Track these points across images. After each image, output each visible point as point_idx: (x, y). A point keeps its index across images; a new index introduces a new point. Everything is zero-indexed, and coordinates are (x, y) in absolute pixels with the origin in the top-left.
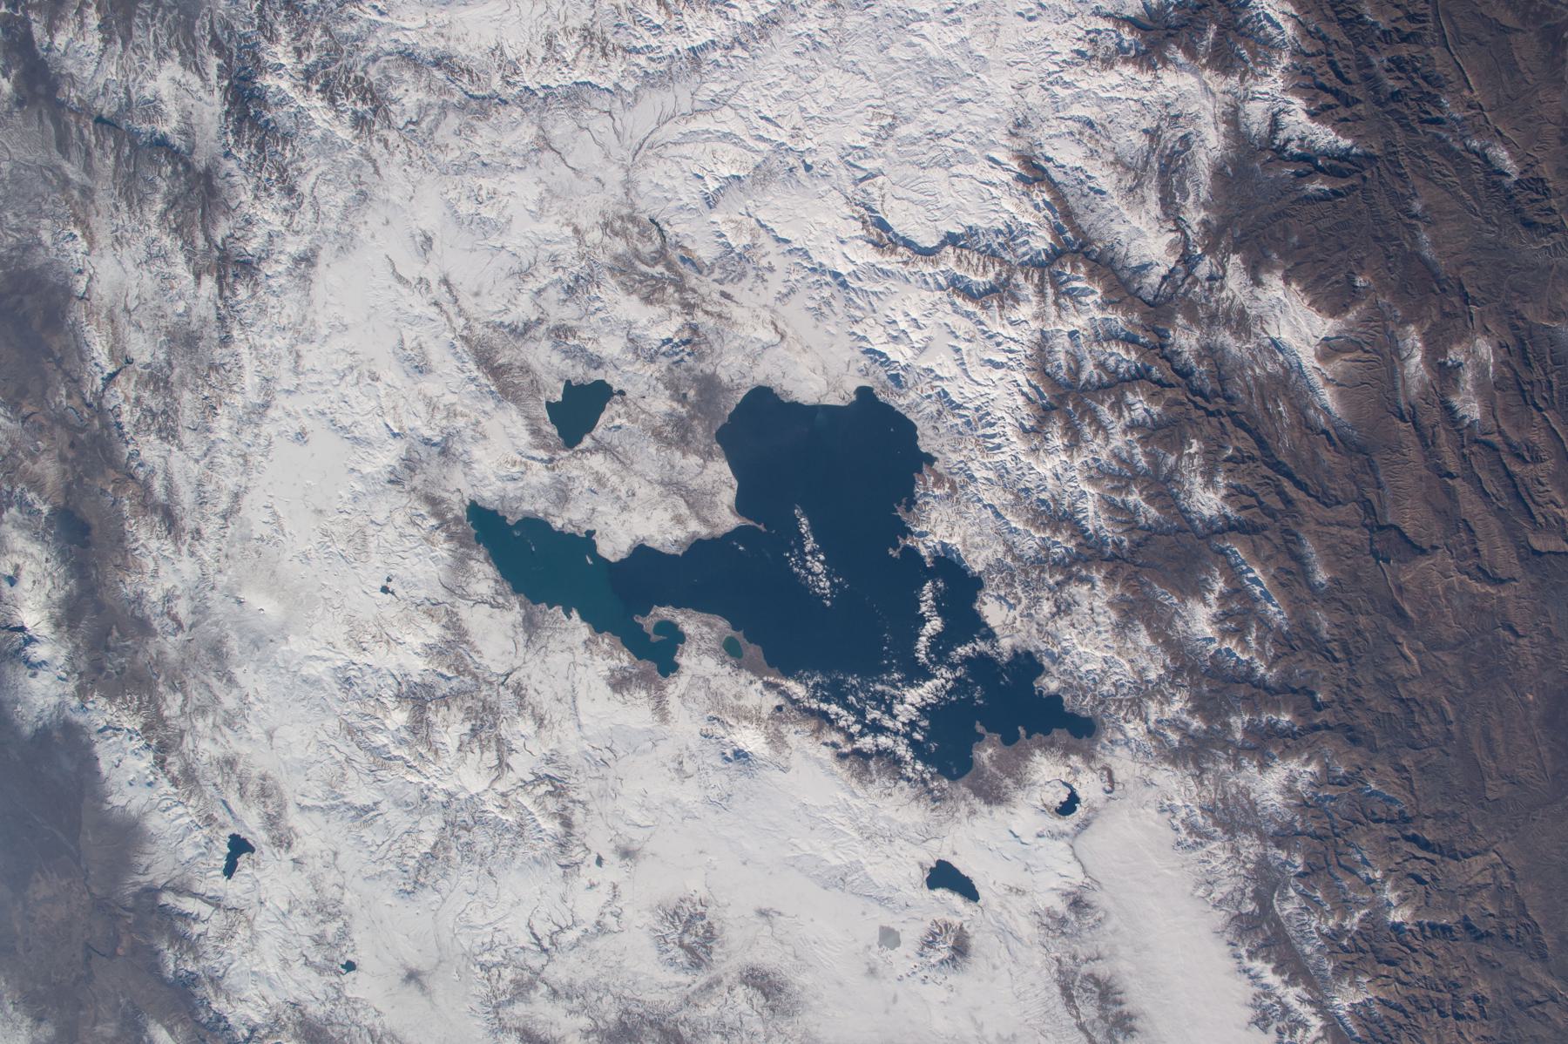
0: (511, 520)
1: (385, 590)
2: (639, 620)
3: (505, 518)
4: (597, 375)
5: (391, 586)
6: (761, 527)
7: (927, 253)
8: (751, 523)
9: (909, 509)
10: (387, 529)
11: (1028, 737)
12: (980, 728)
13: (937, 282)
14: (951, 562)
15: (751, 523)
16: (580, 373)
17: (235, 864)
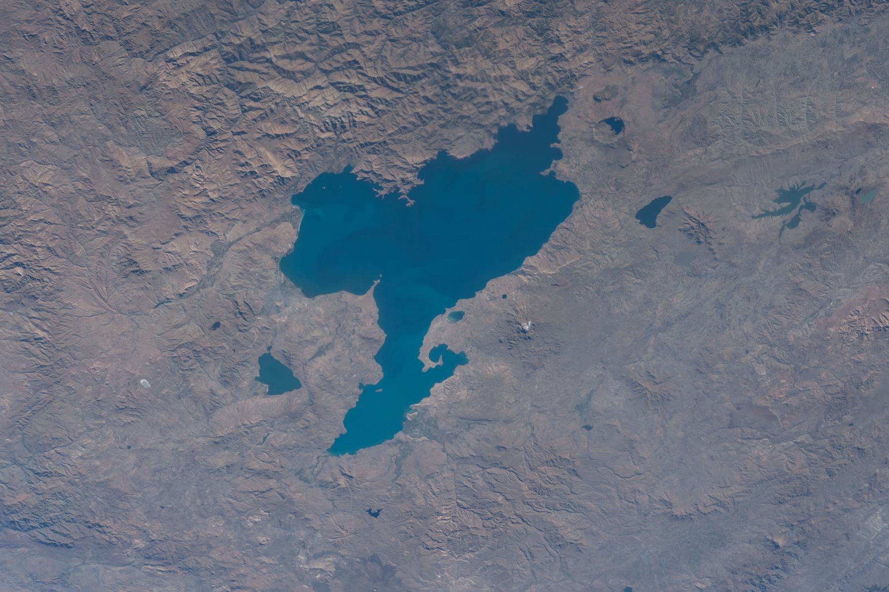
0: (345, 431)
2: (425, 369)
3: (341, 435)
6: (377, 282)
8: (373, 288)
9: (381, 188)
11: (559, 142)
12: (546, 173)
14: (423, 169)
15: (373, 288)
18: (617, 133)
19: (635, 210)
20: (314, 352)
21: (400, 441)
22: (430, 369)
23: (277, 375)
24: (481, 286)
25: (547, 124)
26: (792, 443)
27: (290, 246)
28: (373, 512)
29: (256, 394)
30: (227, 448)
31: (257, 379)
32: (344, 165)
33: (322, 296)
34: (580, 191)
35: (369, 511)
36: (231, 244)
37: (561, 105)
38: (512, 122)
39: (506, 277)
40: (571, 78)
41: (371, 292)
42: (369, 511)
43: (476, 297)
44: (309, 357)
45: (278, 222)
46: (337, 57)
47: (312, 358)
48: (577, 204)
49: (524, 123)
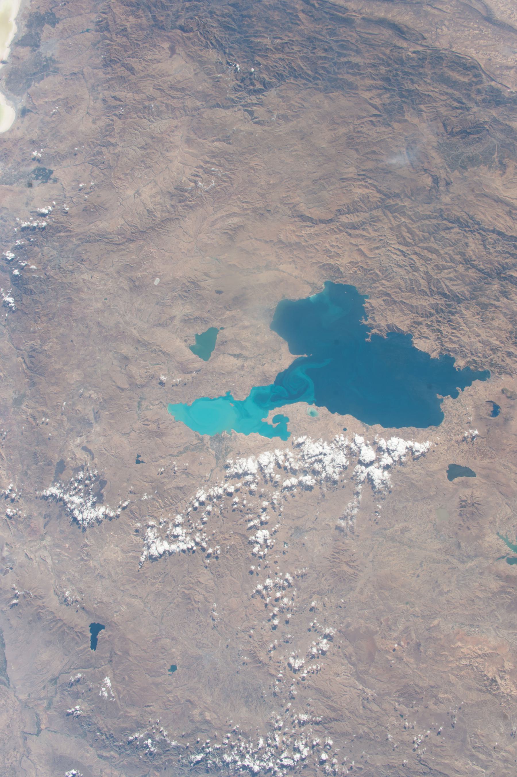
1: (138, 462)
2: (264, 420)
4: (210, 326)
5: (139, 459)
6: (305, 356)
7: (331, 221)
9: (366, 320)
10: (132, 434)
11: (463, 390)
12: (439, 397)
13: (339, 229)
15: (300, 356)
16: (201, 329)
17: (97, 639)
18: (492, 416)
19: (452, 462)
20: (236, 353)
21: (202, 440)
22: (266, 423)
23: (206, 345)
24: (342, 413)
25: (466, 378)
26: (361, 687)
27: (297, 298)
28: (139, 459)
29: (186, 341)
30: (137, 349)
31: (197, 335)
32: (366, 293)
33: (276, 334)
34: (442, 423)
35: (139, 456)
36: (278, 270)
37: (484, 376)
38: (456, 358)
39: (359, 421)
40: (503, 370)
41: (296, 356)
42: (139, 456)
43: (333, 415)
44: (230, 352)
45: (308, 283)
46: (426, 251)
47: (230, 355)
48: (433, 427)
49: (460, 363)
